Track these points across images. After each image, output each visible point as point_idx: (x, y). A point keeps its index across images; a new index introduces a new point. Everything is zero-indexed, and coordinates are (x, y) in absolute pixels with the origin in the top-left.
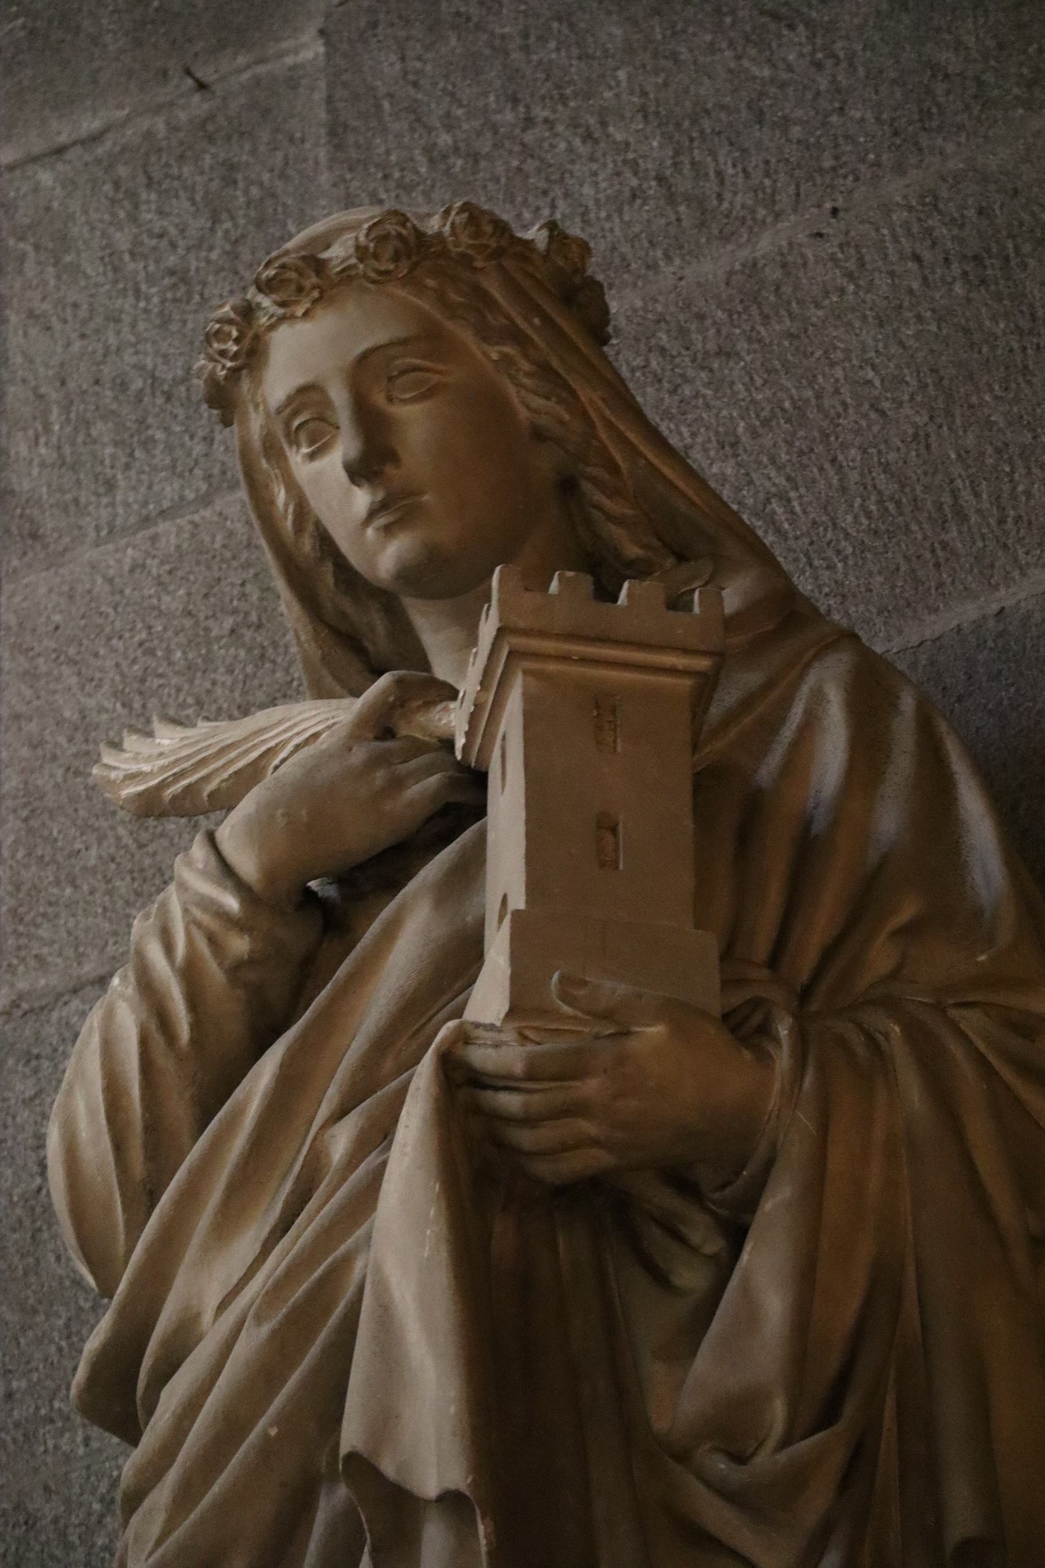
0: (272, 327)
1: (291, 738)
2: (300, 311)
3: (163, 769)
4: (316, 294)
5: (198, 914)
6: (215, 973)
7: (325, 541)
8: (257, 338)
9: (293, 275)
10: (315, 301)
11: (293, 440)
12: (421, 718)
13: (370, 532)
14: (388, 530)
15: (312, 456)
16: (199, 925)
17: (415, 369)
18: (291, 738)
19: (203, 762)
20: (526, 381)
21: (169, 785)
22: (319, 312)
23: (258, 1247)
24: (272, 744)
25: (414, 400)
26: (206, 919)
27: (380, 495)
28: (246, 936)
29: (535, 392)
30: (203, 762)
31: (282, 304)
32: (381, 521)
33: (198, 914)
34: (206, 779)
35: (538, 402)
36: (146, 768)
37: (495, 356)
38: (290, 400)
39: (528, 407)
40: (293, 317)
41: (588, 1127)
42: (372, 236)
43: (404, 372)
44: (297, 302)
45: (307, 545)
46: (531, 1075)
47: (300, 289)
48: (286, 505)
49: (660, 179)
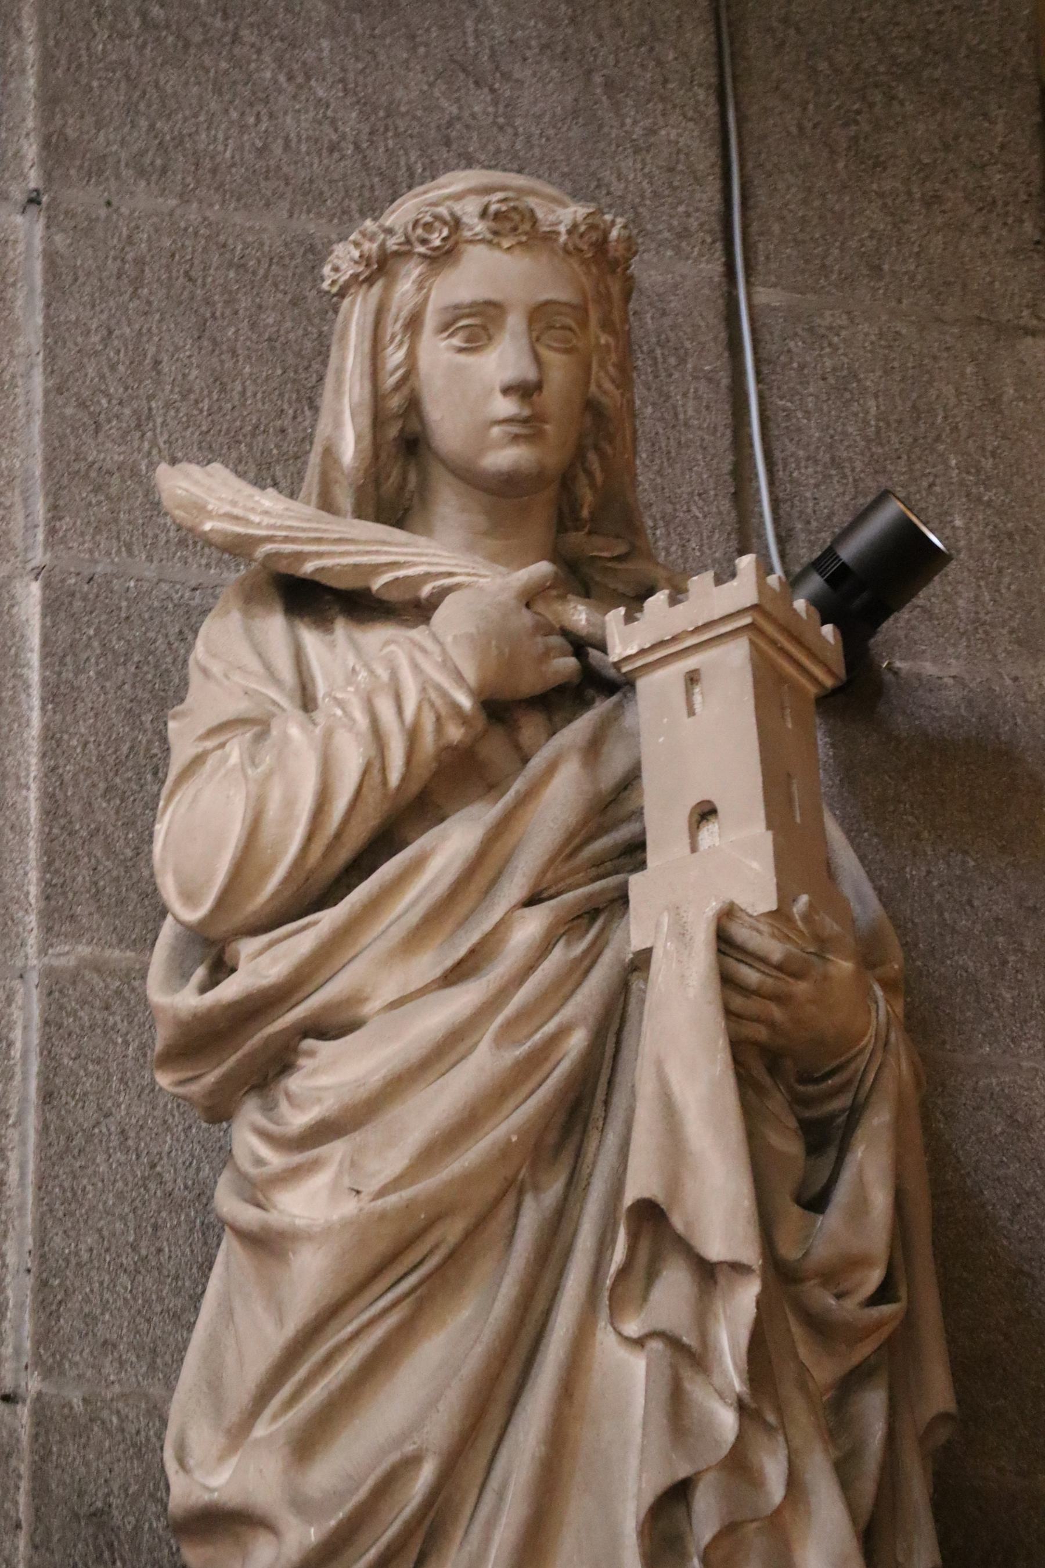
0: (471, 242)
1: (422, 563)
2: (506, 244)
3: (273, 527)
4: (524, 238)
5: (433, 695)
6: (428, 742)
7: (413, 405)
8: (457, 243)
9: (516, 217)
10: (520, 243)
11: (446, 327)
12: (558, 607)
13: (496, 431)
14: (516, 439)
15: (461, 350)
16: (432, 705)
17: (570, 329)
18: (422, 563)
19: (319, 540)
20: (611, 369)
21: (275, 542)
22: (517, 251)
23: (438, 972)
24: (401, 559)
25: (556, 350)
26: (439, 703)
27: (526, 412)
28: (462, 731)
29: (613, 381)
30: (319, 540)
31: (496, 233)
32: (515, 429)
33: (433, 695)
34: (319, 555)
35: (608, 385)
36: (256, 518)
37: (603, 341)
38: (473, 304)
39: (599, 386)
40: (498, 245)
41: (777, 1012)
42: (590, 221)
43: (563, 327)
44: (506, 236)
45: (395, 402)
46: (779, 967)
47: (515, 229)
48: (397, 368)
49: (357, 147)
